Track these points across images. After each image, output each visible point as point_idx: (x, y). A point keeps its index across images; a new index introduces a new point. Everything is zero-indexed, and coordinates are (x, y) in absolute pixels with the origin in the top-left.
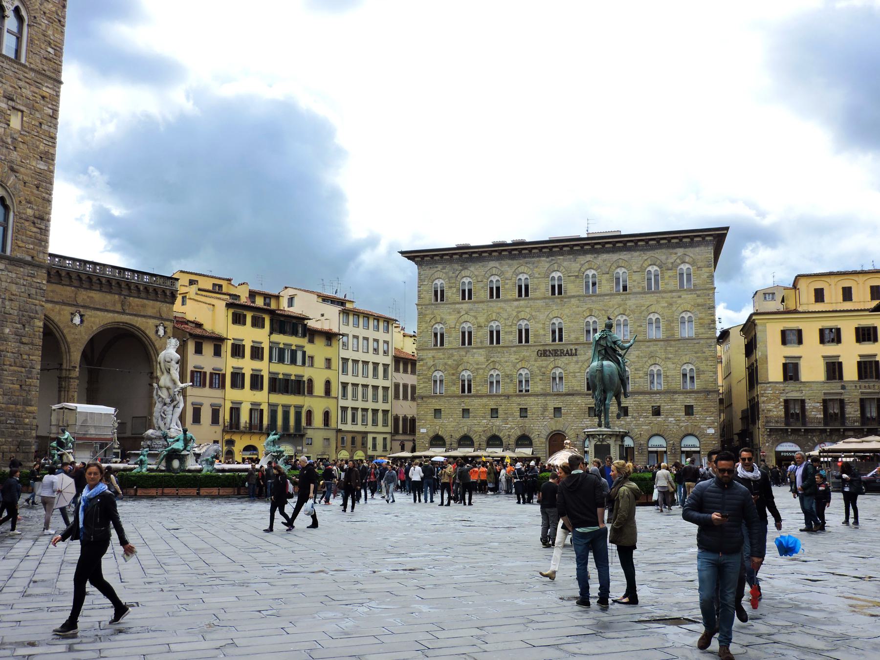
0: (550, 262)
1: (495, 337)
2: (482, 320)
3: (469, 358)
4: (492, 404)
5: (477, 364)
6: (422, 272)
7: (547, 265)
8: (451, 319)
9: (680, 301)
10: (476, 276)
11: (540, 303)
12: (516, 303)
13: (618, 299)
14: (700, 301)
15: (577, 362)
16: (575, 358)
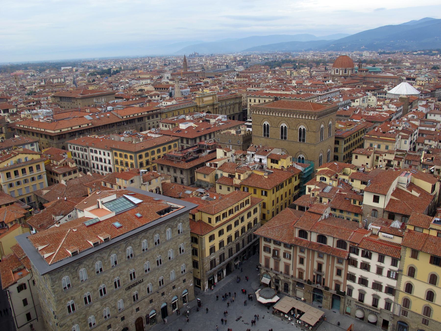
0: (126, 243)
1: (103, 292)
2: (95, 287)
3: (92, 309)
4: (107, 324)
5: (97, 310)
6: (53, 277)
7: (125, 245)
8: (77, 295)
9: (179, 240)
10: (88, 266)
11: (124, 265)
12: (112, 271)
13: (157, 249)
14: (186, 237)
15: (143, 285)
16: (142, 283)
